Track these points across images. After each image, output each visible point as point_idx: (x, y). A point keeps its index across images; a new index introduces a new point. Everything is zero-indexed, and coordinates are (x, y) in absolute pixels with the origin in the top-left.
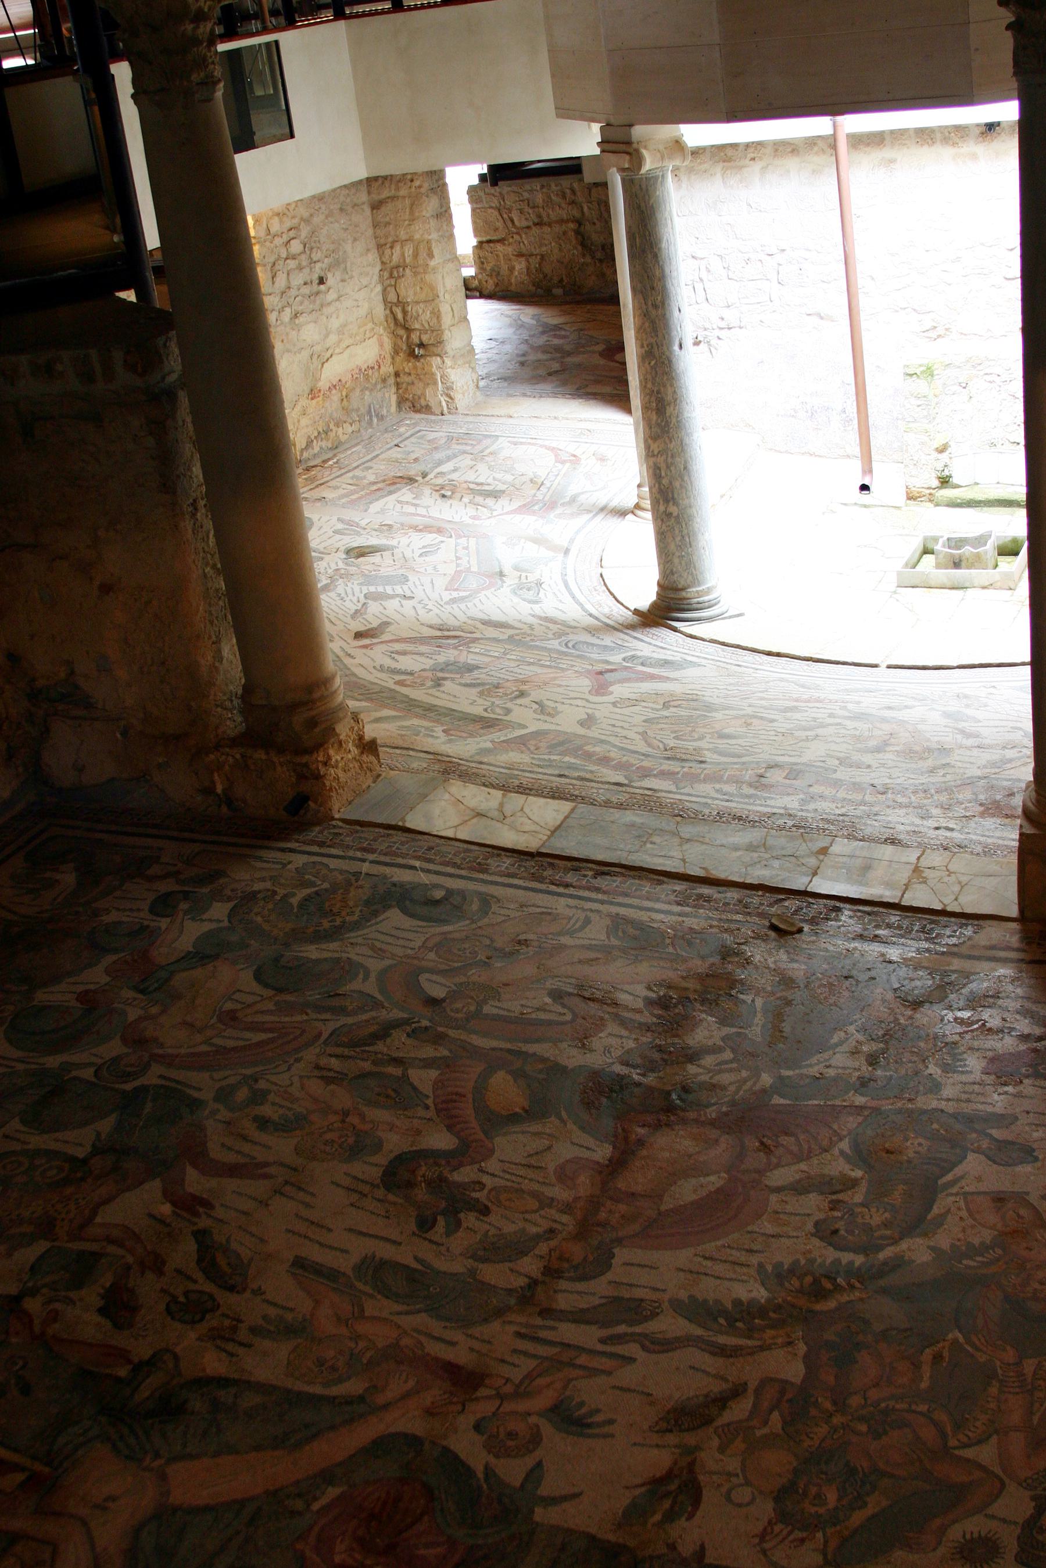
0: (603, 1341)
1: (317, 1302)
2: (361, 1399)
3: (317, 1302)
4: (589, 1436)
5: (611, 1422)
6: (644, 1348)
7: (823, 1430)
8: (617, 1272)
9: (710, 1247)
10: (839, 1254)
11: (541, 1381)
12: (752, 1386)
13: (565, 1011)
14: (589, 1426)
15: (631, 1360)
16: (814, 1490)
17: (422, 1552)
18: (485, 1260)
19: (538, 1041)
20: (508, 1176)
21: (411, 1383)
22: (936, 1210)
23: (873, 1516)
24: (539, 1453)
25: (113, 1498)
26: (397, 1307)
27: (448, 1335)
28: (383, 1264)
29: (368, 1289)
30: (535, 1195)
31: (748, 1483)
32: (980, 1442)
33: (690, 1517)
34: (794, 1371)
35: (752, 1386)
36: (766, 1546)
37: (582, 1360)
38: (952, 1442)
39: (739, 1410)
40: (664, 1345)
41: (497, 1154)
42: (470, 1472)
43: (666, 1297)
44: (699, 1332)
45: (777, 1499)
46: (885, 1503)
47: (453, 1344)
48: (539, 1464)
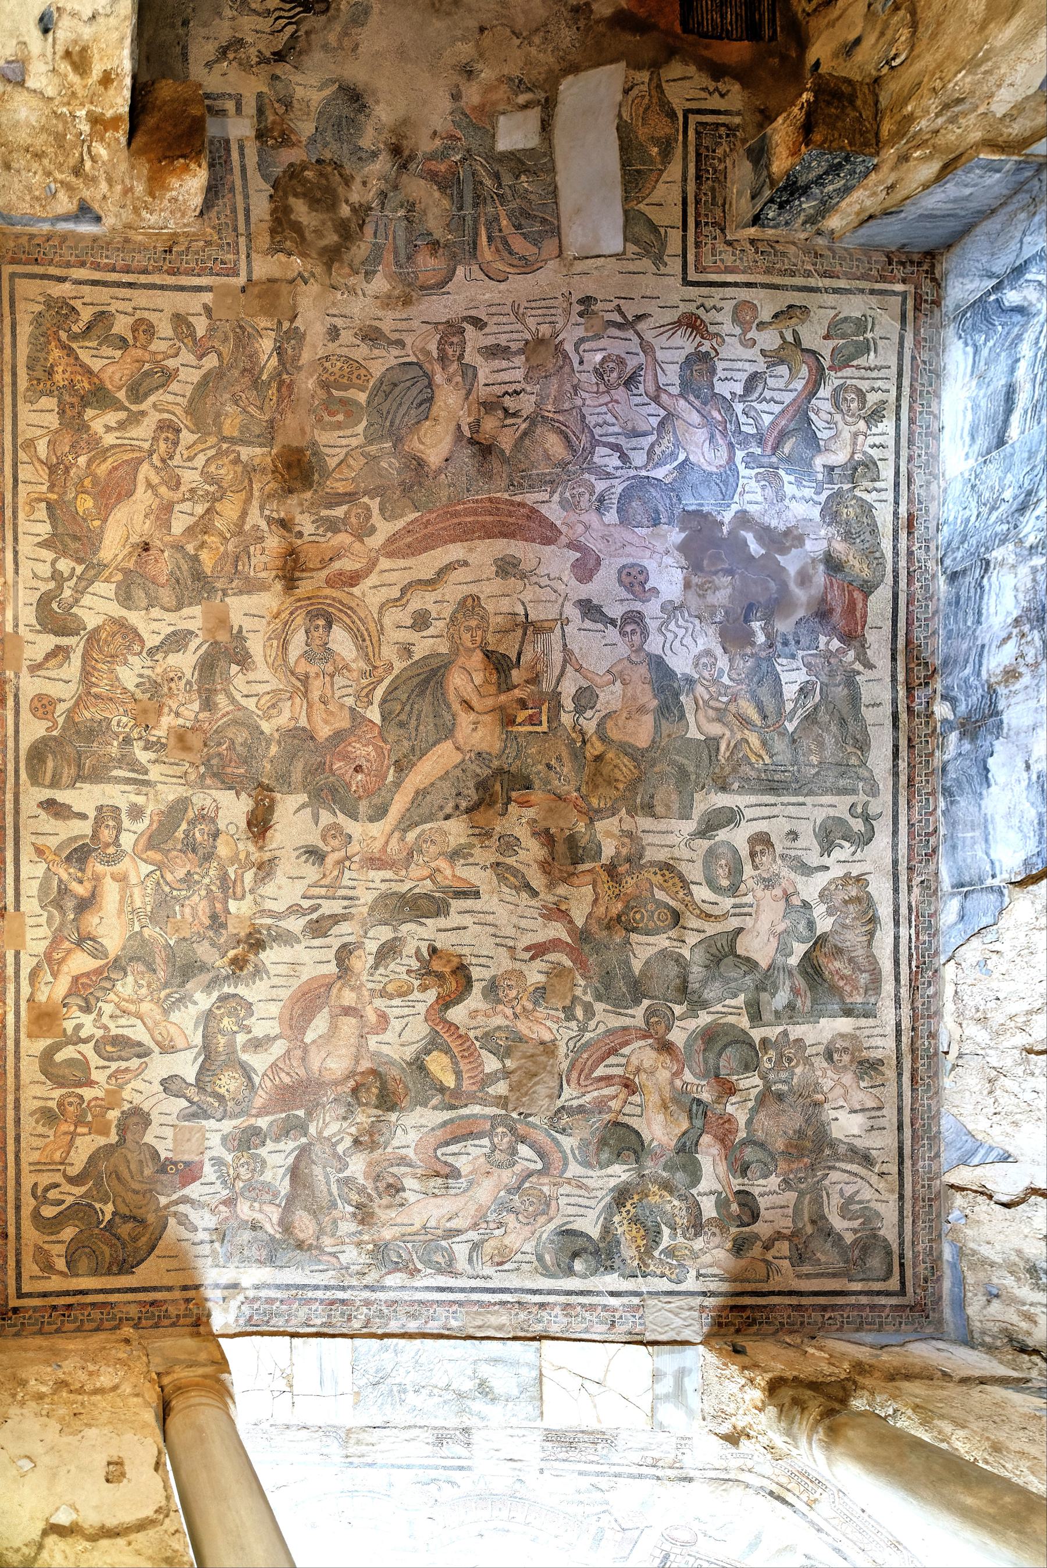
1: (454, 876)
3: (454, 876)
7: (212, 872)
13: (443, 1158)
19: (444, 1124)
22: (201, 1029)
26: (417, 891)
28: (438, 915)
29: (437, 895)
41: (422, 1017)
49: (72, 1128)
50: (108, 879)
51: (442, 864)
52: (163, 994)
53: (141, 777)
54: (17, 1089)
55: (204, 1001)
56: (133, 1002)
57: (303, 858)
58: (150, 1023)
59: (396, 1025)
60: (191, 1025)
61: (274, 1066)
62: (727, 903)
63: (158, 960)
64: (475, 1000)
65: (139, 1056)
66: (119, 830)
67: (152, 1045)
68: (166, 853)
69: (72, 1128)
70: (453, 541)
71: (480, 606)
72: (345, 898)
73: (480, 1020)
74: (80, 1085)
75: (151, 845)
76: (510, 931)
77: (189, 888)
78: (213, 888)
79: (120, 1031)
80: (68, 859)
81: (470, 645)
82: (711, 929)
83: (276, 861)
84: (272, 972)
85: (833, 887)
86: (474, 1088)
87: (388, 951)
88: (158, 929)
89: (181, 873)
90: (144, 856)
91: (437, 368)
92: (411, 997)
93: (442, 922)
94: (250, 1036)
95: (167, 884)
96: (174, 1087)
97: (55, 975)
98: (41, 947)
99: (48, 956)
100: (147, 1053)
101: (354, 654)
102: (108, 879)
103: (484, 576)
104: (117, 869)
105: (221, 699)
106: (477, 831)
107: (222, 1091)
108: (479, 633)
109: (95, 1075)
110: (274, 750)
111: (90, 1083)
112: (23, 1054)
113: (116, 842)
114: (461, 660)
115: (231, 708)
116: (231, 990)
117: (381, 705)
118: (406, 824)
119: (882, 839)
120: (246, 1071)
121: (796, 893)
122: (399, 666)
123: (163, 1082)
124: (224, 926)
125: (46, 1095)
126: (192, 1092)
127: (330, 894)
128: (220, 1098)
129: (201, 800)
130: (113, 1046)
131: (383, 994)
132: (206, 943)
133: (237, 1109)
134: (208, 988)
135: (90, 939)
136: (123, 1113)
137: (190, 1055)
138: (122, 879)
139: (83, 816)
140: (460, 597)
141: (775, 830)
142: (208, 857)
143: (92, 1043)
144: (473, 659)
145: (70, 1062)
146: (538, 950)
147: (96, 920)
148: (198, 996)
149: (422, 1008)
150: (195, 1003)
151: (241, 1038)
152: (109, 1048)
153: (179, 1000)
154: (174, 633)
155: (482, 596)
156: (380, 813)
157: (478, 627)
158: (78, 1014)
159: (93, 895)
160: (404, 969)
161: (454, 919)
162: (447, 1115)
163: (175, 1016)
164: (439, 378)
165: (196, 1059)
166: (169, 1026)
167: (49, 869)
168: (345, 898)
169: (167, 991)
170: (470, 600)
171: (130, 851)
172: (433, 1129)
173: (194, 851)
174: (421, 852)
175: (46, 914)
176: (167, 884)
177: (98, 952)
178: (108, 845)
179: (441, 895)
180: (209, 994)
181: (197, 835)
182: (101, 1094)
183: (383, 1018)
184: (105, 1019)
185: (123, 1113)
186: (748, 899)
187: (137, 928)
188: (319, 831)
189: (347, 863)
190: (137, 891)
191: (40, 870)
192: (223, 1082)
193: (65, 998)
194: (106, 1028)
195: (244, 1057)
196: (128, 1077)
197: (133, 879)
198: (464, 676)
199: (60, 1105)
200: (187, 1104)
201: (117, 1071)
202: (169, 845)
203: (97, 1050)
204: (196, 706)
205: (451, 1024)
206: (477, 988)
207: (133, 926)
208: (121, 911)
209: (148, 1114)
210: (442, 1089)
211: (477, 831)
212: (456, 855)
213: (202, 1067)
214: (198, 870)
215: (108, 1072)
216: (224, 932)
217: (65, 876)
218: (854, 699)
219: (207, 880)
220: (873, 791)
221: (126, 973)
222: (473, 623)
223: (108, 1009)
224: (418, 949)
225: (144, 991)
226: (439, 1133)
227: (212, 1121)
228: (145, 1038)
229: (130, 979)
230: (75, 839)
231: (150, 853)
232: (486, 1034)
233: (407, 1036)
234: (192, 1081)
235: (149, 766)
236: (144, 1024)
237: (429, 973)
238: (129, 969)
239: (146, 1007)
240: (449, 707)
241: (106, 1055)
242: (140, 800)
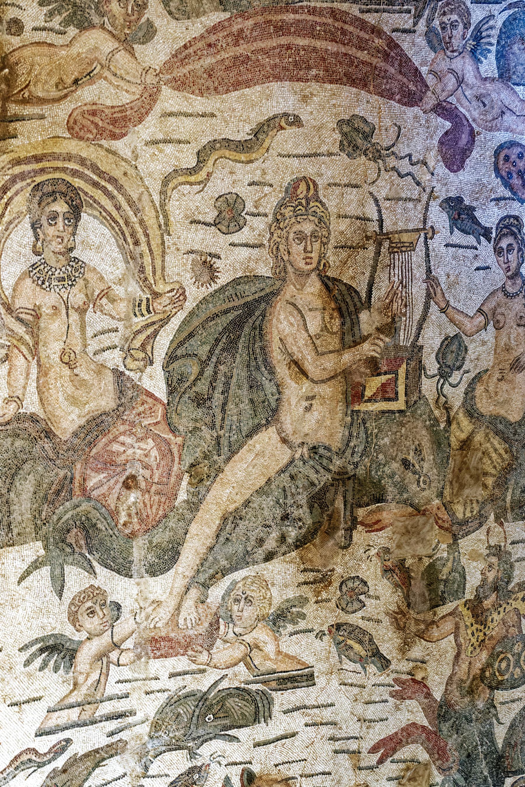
2: (206, 586)
17: (102, 476)
21: (181, 621)
24: (65, 607)
25: (308, 409)
70: (278, 78)
71: (318, 200)
81: (301, 264)
103: (324, 149)
106: (311, 576)
108: (317, 246)
114: (290, 291)
140: (288, 179)
144: (309, 289)
155: (320, 182)
157: (313, 235)
170: (303, 187)
198: (295, 319)
211: (311, 576)
222: (308, 228)
240: (272, 372)
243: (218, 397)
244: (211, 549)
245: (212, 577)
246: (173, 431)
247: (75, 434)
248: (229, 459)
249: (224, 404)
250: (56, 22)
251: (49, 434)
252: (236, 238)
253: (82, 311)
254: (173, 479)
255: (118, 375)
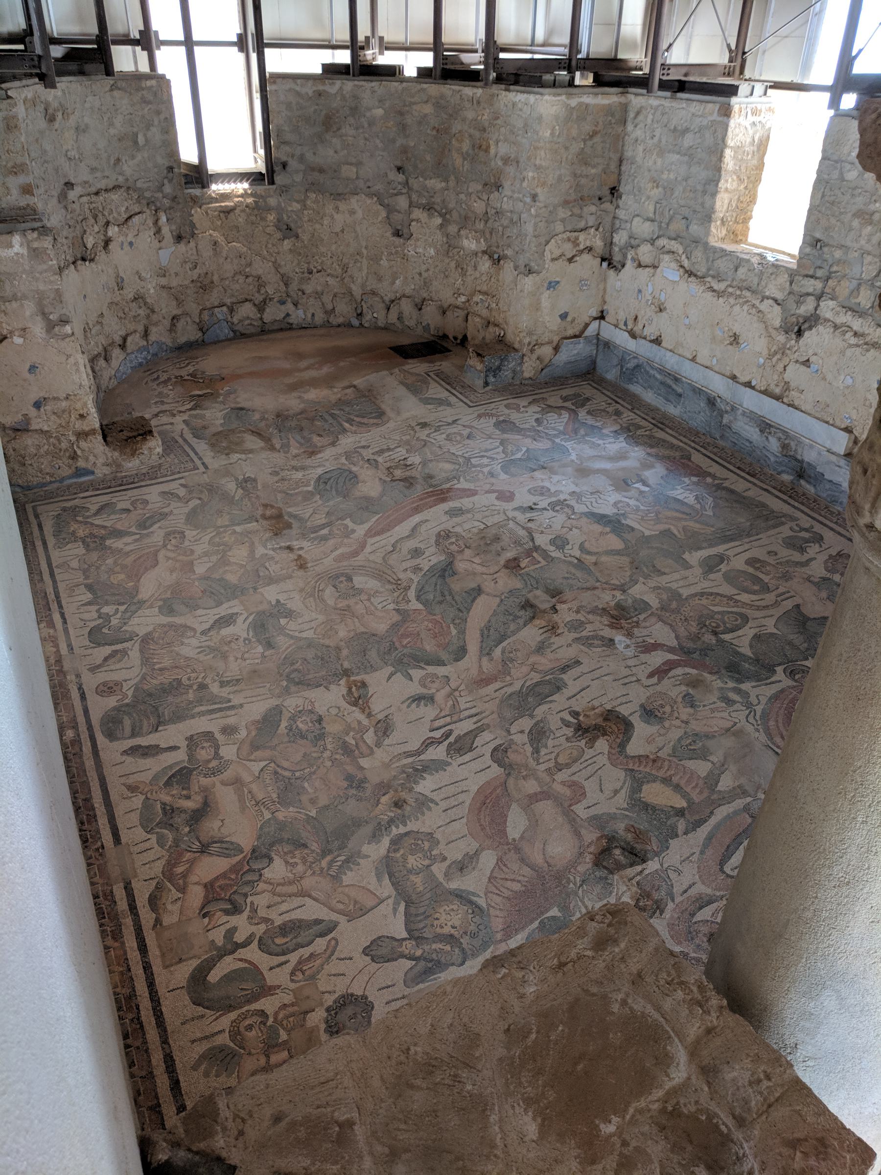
0: (451, 731)
1: (551, 661)
4: (409, 698)
5: (408, 707)
6: (432, 738)
7: (329, 747)
8: (487, 760)
9: (468, 799)
10: (408, 829)
11: (451, 702)
12: (375, 749)
14: (414, 701)
15: (432, 730)
16: (310, 725)
18: (536, 724)
19: (709, 838)
20: (590, 762)
21: (485, 670)
23: (279, 726)
26: (528, 684)
27: (503, 691)
29: (547, 678)
30: (568, 766)
31: (336, 715)
32: (262, 770)
33: (343, 695)
34: (364, 762)
35: (375, 749)
36: (307, 701)
37: (448, 719)
38: (272, 765)
39: (370, 737)
40: (429, 743)
41: (608, 765)
42: (428, 664)
43: (454, 763)
44: (422, 757)
45: (320, 716)
46: (279, 732)
47: (496, 691)
48: (411, 680)
49: (263, 1061)
50: (218, 784)
51: (533, 659)
52: (324, 863)
53: (228, 705)
54: (165, 1041)
55: (378, 850)
56: (291, 883)
57: (414, 705)
58: (321, 896)
59: (590, 786)
60: (374, 880)
61: (491, 878)
62: (770, 598)
63: (304, 834)
64: (642, 730)
65: (322, 935)
66: (217, 747)
67: (334, 917)
68: (273, 748)
69: (263, 1061)
70: (411, 516)
72: (469, 717)
73: (660, 742)
74: (255, 998)
75: (255, 747)
76: (627, 672)
77: (311, 766)
78: (338, 757)
79: (287, 917)
80: (168, 784)
82: (778, 612)
83: (390, 717)
84: (437, 799)
85: (830, 565)
86: (705, 794)
87: (538, 735)
88: (291, 809)
89: (299, 756)
90: (252, 757)
91: (352, 466)
92: (586, 757)
93: (567, 692)
94: (448, 863)
95: (285, 769)
96: (383, 951)
97: (183, 890)
98: (159, 866)
99: (168, 873)
100: (332, 927)
101: (379, 584)
102: (218, 784)
104: (228, 774)
105: (282, 641)
106: (545, 629)
107: (447, 930)
109: (271, 979)
110: (345, 652)
111: (267, 990)
112: (162, 991)
113: (217, 756)
114: (459, 557)
115: (292, 641)
116: (402, 830)
117: (417, 600)
118: (486, 652)
119: (828, 535)
120: (462, 897)
121: (810, 576)
122: (416, 579)
123: (366, 952)
124: (364, 780)
125: (208, 1031)
126: (409, 947)
127: (455, 718)
128: (450, 939)
129: (292, 703)
130: (284, 936)
131: (559, 767)
132: (352, 802)
133: (477, 943)
134: (375, 837)
135: (216, 842)
136: (328, 1010)
137: (386, 908)
138: (237, 782)
139: (174, 748)
141: (758, 553)
142: (321, 736)
143: (255, 944)
145: (229, 978)
146: (661, 672)
147: (216, 824)
148: (366, 849)
149: (603, 760)
150: (368, 856)
151: (438, 870)
152: (278, 941)
153: (347, 861)
154: (220, 618)
156: (461, 653)
158: (225, 918)
159: (206, 803)
160: (563, 739)
161: (573, 687)
162: (704, 831)
163: (349, 878)
164: (354, 469)
165: (395, 910)
166: (347, 890)
167: (147, 798)
168: (469, 717)
169: (329, 858)
171: (234, 758)
172: (702, 852)
173: (303, 737)
174: (512, 660)
175: (154, 838)
176: (285, 769)
177: (229, 849)
178: (209, 761)
179: (551, 676)
180: (379, 841)
181: (301, 725)
182: (288, 999)
183: (572, 785)
184: (262, 913)
185: (328, 1010)
186: (781, 590)
187: (267, 815)
188: (417, 683)
189: (457, 694)
190: (254, 787)
191: (138, 801)
192: (442, 920)
193: (203, 908)
194: (266, 920)
195: (453, 885)
196: (319, 962)
197: (247, 778)
199: (235, 1034)
200: (409, 964)
201: (300, 962)
202: (275, 741)
203: (263, 946)
204: (260, 649)
205: (639, 757)
206: (635, 720)
207: (262, 815)
208: (243, 809)
209: (365, 997)
210: (680, 813)
211: (545, 629)
212: (540, 649)
213: (407, 914)
214: (314, 749)
215: (289, 967)
216: (367, 785)
217: (167, 799)
218: (732, 492)
219: (327, 754)
220: (793, 519)
221: (271, 860)
223: (261, 901)
224: (562, 720)
225: (300, 868)
226: (709, 852)
227: (451, 968)
228: (323, 913)
229: (278, 862)
230: (170, 767)
231: (259, 754)
232: (674, 749)
233: (609, 787)
234: (405, 935)
235: (231, 696)
236: (315, 899)
237: (586, 731)
238: (273, 855)
239: (308, 883)
241: (279, 950)
242: (231, 721)
243: (448, 598)
244: (482, 642)
245: (490, 649)
246: (435, 615)
247: (387, 632)
248: (468, 613)
249: (453, 598)
250: (315, 543)
251: (374, 635)
252: (424, 557)
253: (369, 600)
254: (445, 629)
255: (397, 610)
